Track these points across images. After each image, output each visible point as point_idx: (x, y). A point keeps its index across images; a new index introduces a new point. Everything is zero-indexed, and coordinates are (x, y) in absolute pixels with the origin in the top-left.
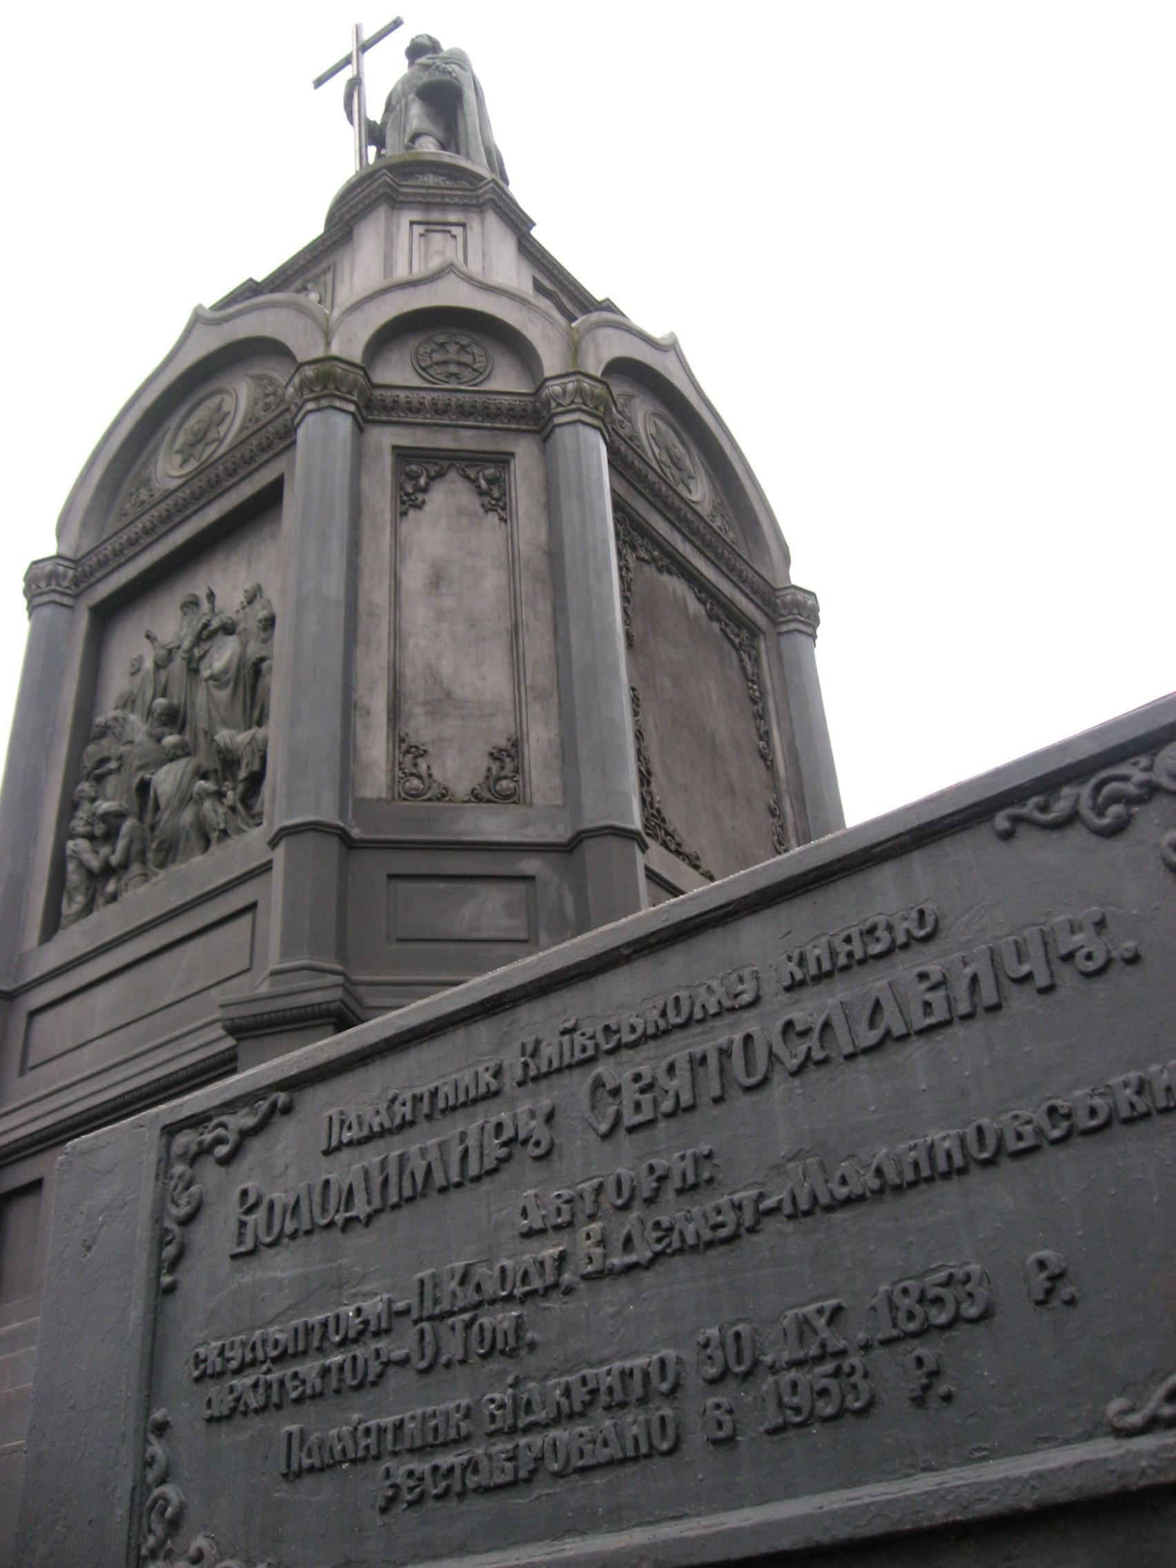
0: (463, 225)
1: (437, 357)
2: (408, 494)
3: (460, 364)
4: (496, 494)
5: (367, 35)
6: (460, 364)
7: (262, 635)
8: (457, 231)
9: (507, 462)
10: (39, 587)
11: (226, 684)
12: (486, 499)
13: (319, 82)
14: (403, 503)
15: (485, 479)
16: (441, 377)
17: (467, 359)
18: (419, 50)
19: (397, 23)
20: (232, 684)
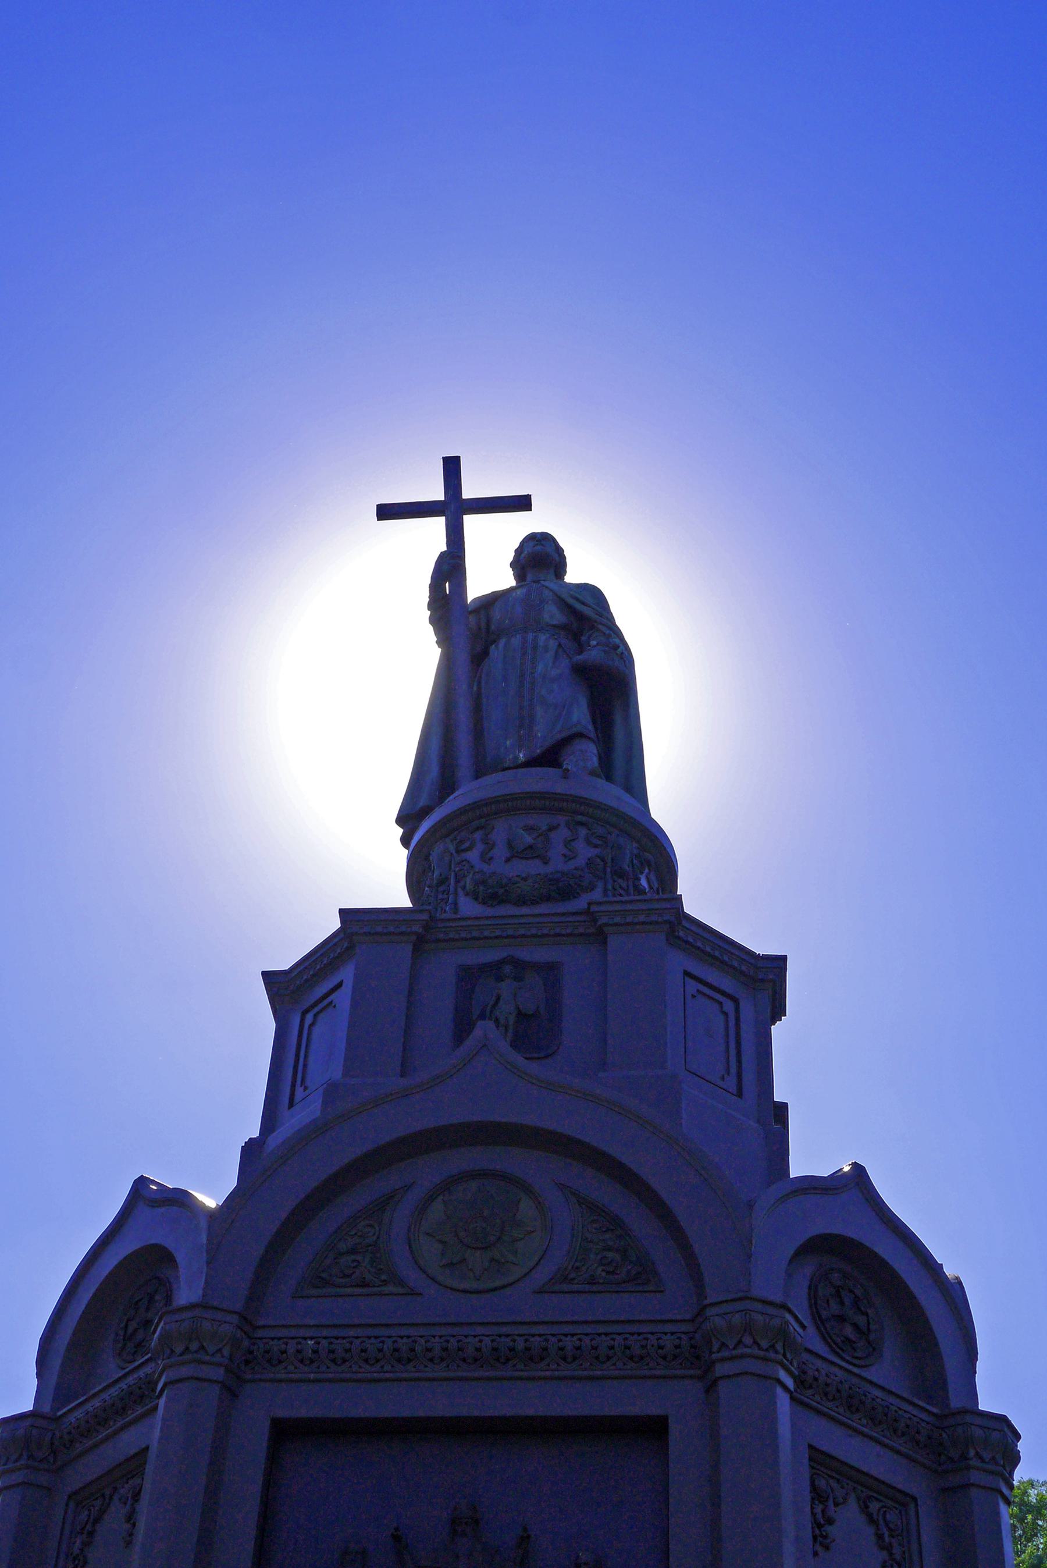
0: (736, 1001)
1: (835, 1308)
2: (820, 1526)
3: (855, 1326)
4: (897, 1551)
5: (469, 491)
6: (855, 1326)
8: (729, 1006)
9: (905, 1505)
12: (884, 1555)
13: (386, 512)
14: (815, 1538)
15: (890, 1529)
16: (838, 1340)
17: (861, 1320)
18: (539, 557)
19: (522, 503)
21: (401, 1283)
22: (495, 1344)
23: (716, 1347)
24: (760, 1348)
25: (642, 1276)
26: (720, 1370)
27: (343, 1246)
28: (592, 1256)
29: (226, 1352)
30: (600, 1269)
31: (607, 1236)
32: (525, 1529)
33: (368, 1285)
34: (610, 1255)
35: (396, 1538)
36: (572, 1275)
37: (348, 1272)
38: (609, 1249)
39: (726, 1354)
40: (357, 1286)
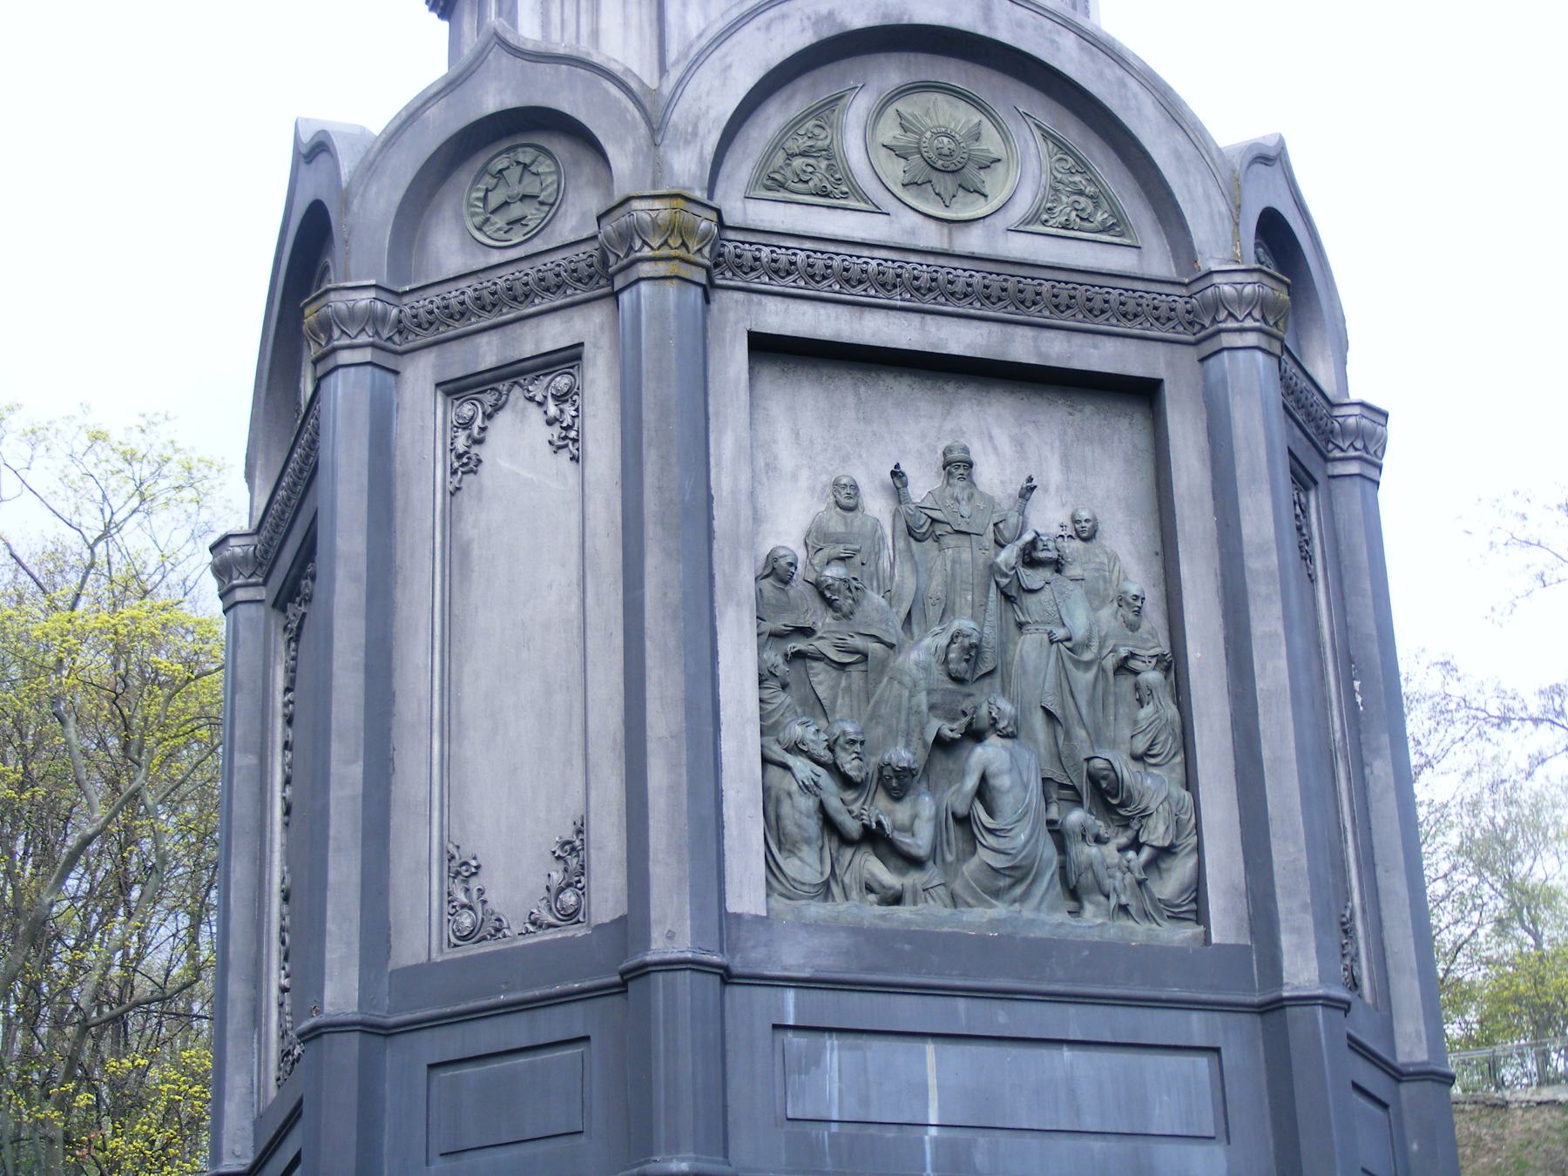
7: (1131, 616)
10: (684, 244)
11: (1088, 665)
20: (1094, 670)
21: (865, 198)
22: (987, 282)
23: (1223, 315)
24: (1266, 322)
25: (1116, 227)
26: (1227, 340)
27: (793, 146)
28: (1064, 199)
29: (706, 251)
30: (1074, 214)
31: (1077, 178)
32: (1030, 479)
33: (827, 196)
34: (1082, 199)
35: (897, 474)
36: (1045, 217)
37: (805, 178)
38: (1081, 193)
39: (1231, 324)
40: (817, 194)
